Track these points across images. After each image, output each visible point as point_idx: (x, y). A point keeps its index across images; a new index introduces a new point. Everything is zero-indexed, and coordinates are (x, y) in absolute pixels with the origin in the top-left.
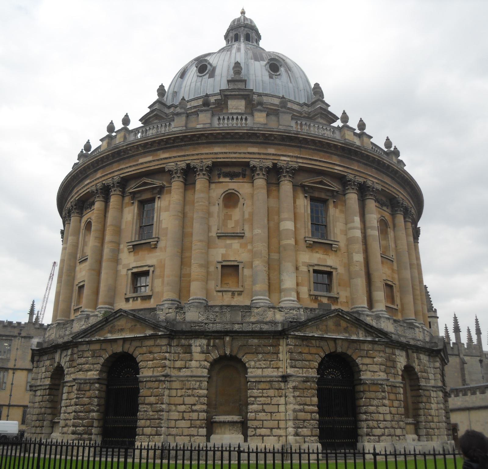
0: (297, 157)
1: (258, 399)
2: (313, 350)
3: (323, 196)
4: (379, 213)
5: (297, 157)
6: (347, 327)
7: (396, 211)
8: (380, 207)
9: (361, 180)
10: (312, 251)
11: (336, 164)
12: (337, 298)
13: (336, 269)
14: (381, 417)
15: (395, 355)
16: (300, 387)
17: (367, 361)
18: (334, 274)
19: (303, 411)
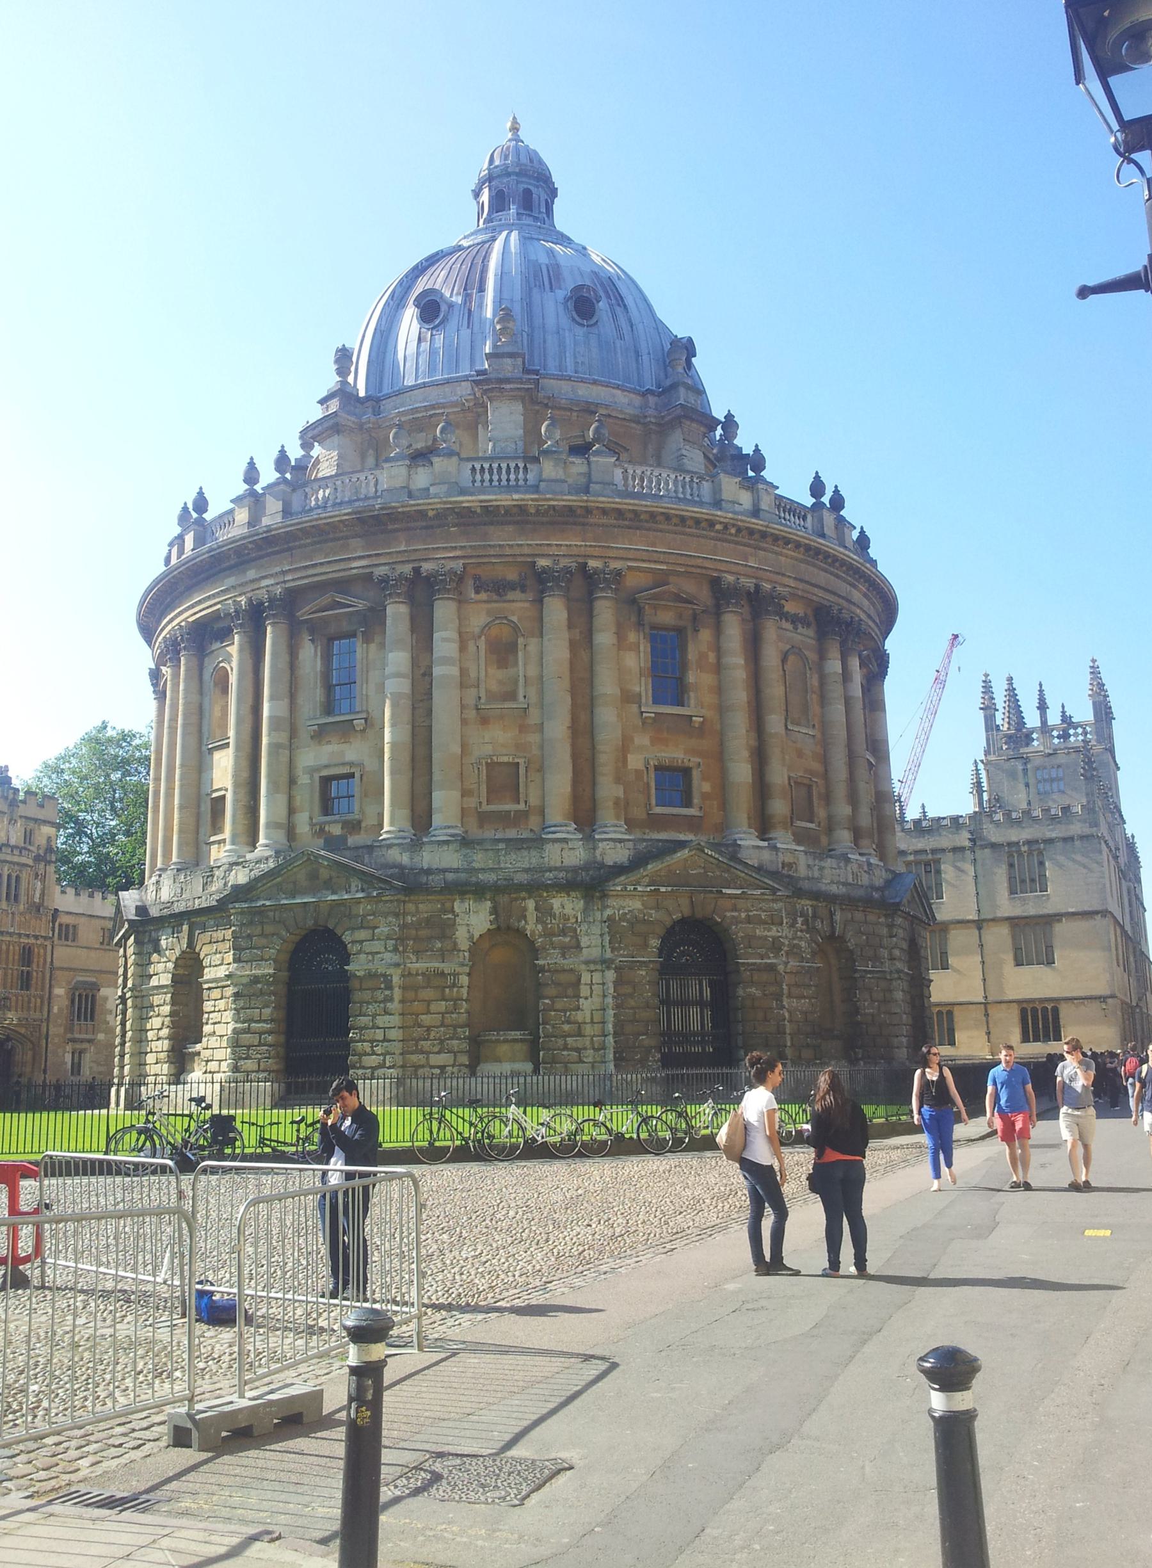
0: (284, 573)
1: (211, 1015)
2: (269, 929)
3: (345, 626)
4: (489, 613)
5: (284, 573)
6: (331, 878)
7: (542, 592)
8: (495, 597)
9: (407, 569)
10: (319, 743)
11: (357, 559)
12: (360, 822)
13: (361, 765)
14: (379, 1034)
15: (452, 911)
16: (245, 992)
17: (362, 934)
18: (357, 775)
19: (248, 1031)
